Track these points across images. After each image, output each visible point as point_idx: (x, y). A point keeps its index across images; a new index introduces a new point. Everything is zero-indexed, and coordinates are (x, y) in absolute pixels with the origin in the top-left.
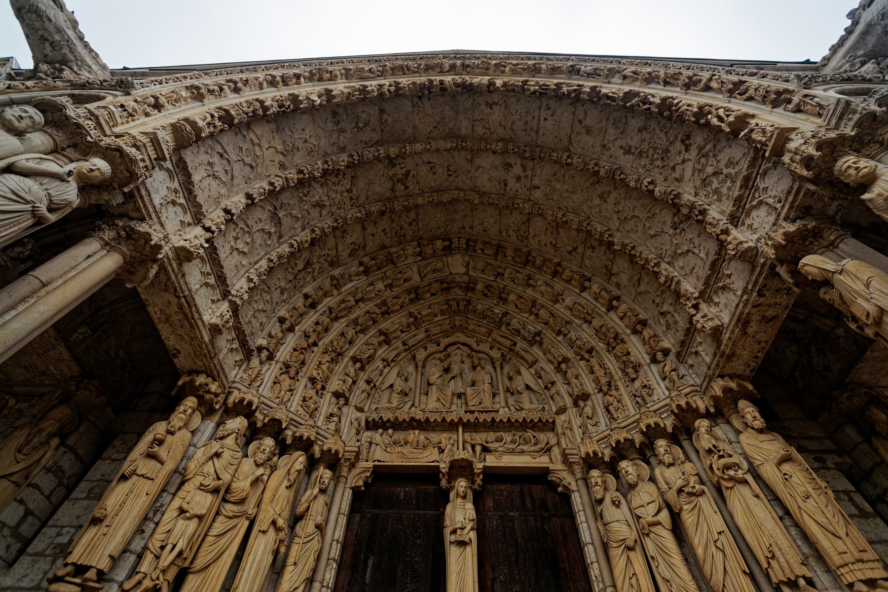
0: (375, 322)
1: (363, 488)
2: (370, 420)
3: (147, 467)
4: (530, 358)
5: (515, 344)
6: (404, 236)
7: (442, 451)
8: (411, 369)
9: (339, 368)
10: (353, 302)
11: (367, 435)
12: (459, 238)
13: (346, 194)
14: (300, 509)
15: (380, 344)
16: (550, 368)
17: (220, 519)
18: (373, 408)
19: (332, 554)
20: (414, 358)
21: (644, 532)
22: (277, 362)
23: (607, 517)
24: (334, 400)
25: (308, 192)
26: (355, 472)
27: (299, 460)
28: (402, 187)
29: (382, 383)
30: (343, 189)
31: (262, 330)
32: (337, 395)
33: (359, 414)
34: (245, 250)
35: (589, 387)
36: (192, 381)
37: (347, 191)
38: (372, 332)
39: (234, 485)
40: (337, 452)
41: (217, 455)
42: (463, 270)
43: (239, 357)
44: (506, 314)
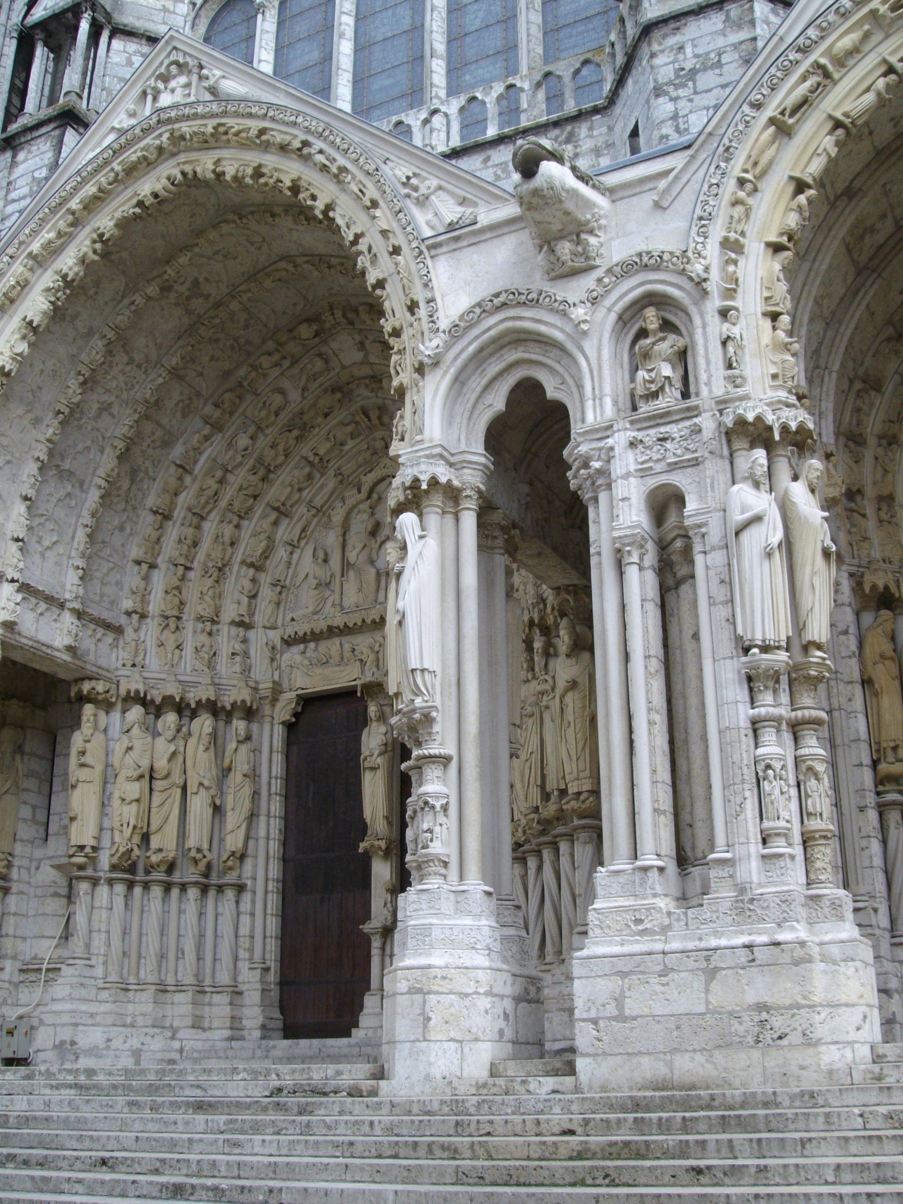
0: (255, 497)
1: (294, 720)
2: (286, 637)
3: (83, 774)
6: (248, 342)
9: (229, 584)
10: (215, 486)
12: (331, 308)
13: (128, 368)
14: (226, 763)
15: (276, 523)
17: (155, 794)
18: (288, 618)
19: (273, 790)
22: (153, 617)
24: (234, 630)
25: (82, 413)
26: (279, 705)
27: (204, 724)
28: (201, 300)
29: (295, 575)
30: (121, 367)
31: (122, 589)
33: (271, 633)
34: (55, 539)
36: (80, 691)
37: (127, 364)
38: (259, 510)
39: (156, 766)
40: (243, 701)
41: (130, 749)
43: (110, 638)
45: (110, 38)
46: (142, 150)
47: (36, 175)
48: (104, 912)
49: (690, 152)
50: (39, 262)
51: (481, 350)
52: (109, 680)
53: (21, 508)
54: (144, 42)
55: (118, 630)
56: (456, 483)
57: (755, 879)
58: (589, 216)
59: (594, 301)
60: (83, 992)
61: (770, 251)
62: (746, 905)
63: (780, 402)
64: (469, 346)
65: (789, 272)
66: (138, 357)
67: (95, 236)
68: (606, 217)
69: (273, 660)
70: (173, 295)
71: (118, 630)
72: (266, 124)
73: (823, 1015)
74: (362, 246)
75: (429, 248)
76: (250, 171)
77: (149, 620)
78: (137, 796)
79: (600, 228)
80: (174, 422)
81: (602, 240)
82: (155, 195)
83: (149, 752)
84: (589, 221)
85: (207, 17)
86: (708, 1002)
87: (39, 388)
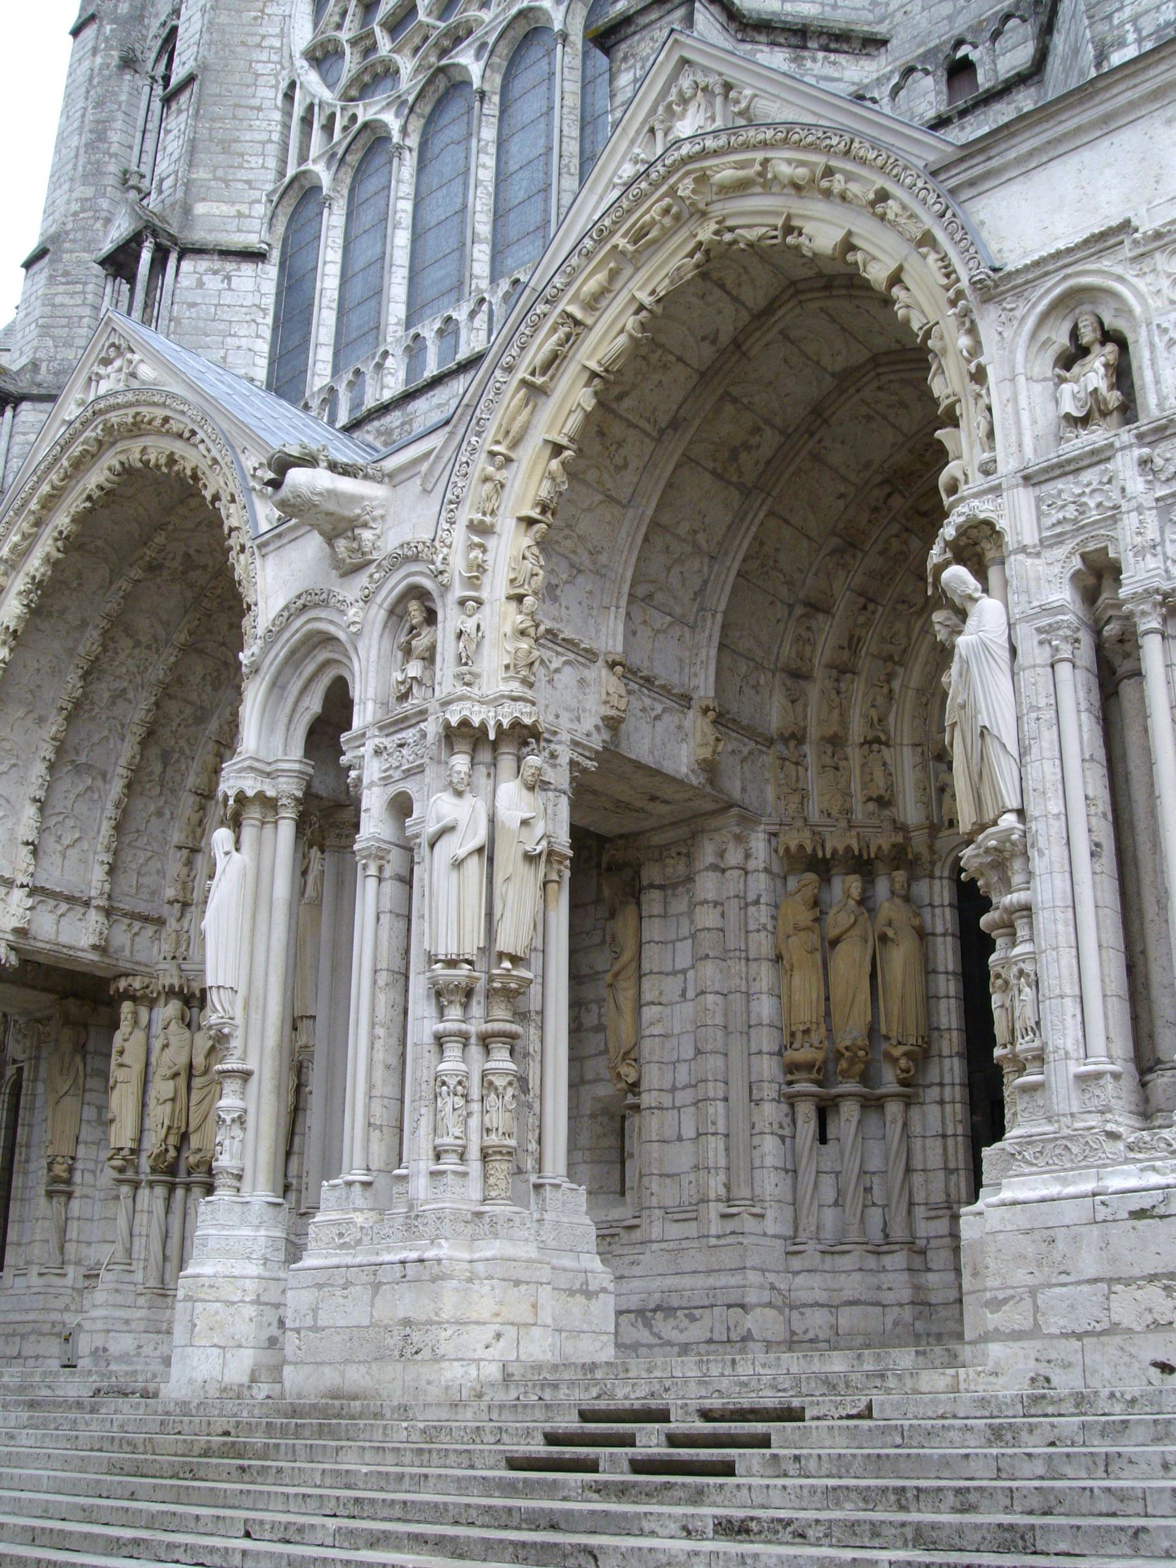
13: (137, 651)
25: (92, 703)
28: (199, 572)
30: (127, 651)
34: (77, 836)
41: (166, 1046)
43: (150, 930)
45: (179, 260)
46: (83, 443)
48: (145, 1215)
49: (448, 429)
51: (293, 652)
52: (150, 975)
53: (31, 810)
54: (216, 257)
55: (160, 922)
56: (271, 793)
57: (422, 1196)
58: (358, 511)
59: (367, 599)
60: (120, 1299)
61: (523, 525)
62: (413, 1220)
63: (503, 696)
64: (280, 652)
65: (543, 544)
66: (144, 640)
67: (56, 534)
68: (382, 506)
70: (166, 572)
71: (160, 922)
72: (168, 413)
73: (449, 1332)
75: (260, 547)
76: (163, 461)
77: (193, 908)
78: (171, 1095)
79: (374, 519)
80: (205, 697)
81: (378, 532)
83: (187, 1049)
84: (359, 516)
85: (284, 214)
86: (372, 1316)
87: (39, 686)
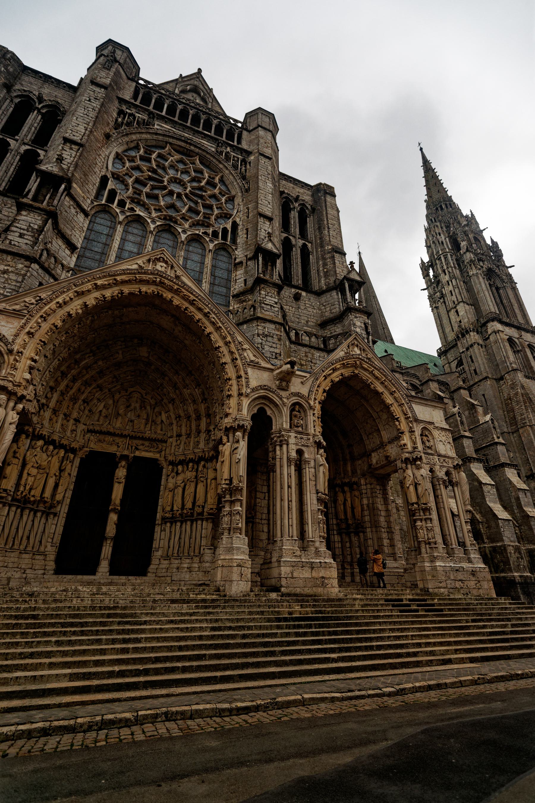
3: (15, 461)
4: (167, 409)
5: (162, 400)
7: (118, 447)
8: (111, 402)
9: (77, 406)
10: (85, 373)
11: (88, 435)
15: (97, 392)
16: (173, 416)
20: (113, 396)
21: (176, 487)
23: (169, 481)
24: (74, 422)
26: (82, 452)
32: (75, 420)
33: (84, 426)
35: (183, 432)
41: (36, 455)
42: (146, 355)
44: (162, 384)
47: (32, 225)
50: (97, 287)
69: (84, 436)
74: (221, 350)
82: (146, 293)
